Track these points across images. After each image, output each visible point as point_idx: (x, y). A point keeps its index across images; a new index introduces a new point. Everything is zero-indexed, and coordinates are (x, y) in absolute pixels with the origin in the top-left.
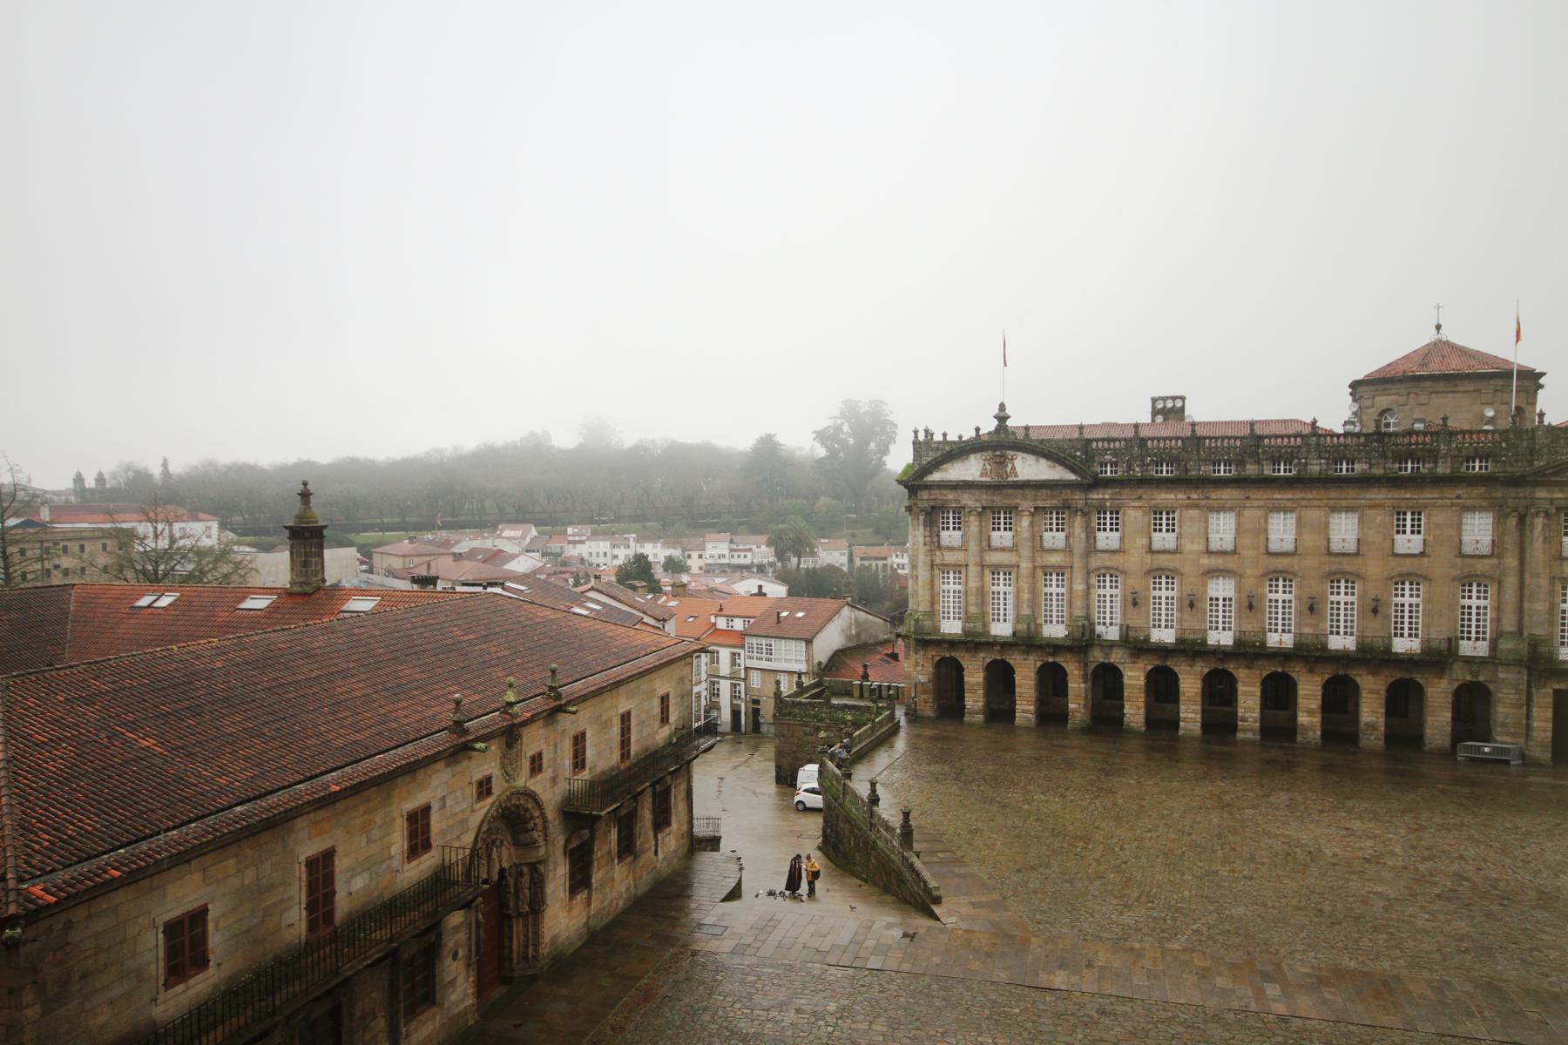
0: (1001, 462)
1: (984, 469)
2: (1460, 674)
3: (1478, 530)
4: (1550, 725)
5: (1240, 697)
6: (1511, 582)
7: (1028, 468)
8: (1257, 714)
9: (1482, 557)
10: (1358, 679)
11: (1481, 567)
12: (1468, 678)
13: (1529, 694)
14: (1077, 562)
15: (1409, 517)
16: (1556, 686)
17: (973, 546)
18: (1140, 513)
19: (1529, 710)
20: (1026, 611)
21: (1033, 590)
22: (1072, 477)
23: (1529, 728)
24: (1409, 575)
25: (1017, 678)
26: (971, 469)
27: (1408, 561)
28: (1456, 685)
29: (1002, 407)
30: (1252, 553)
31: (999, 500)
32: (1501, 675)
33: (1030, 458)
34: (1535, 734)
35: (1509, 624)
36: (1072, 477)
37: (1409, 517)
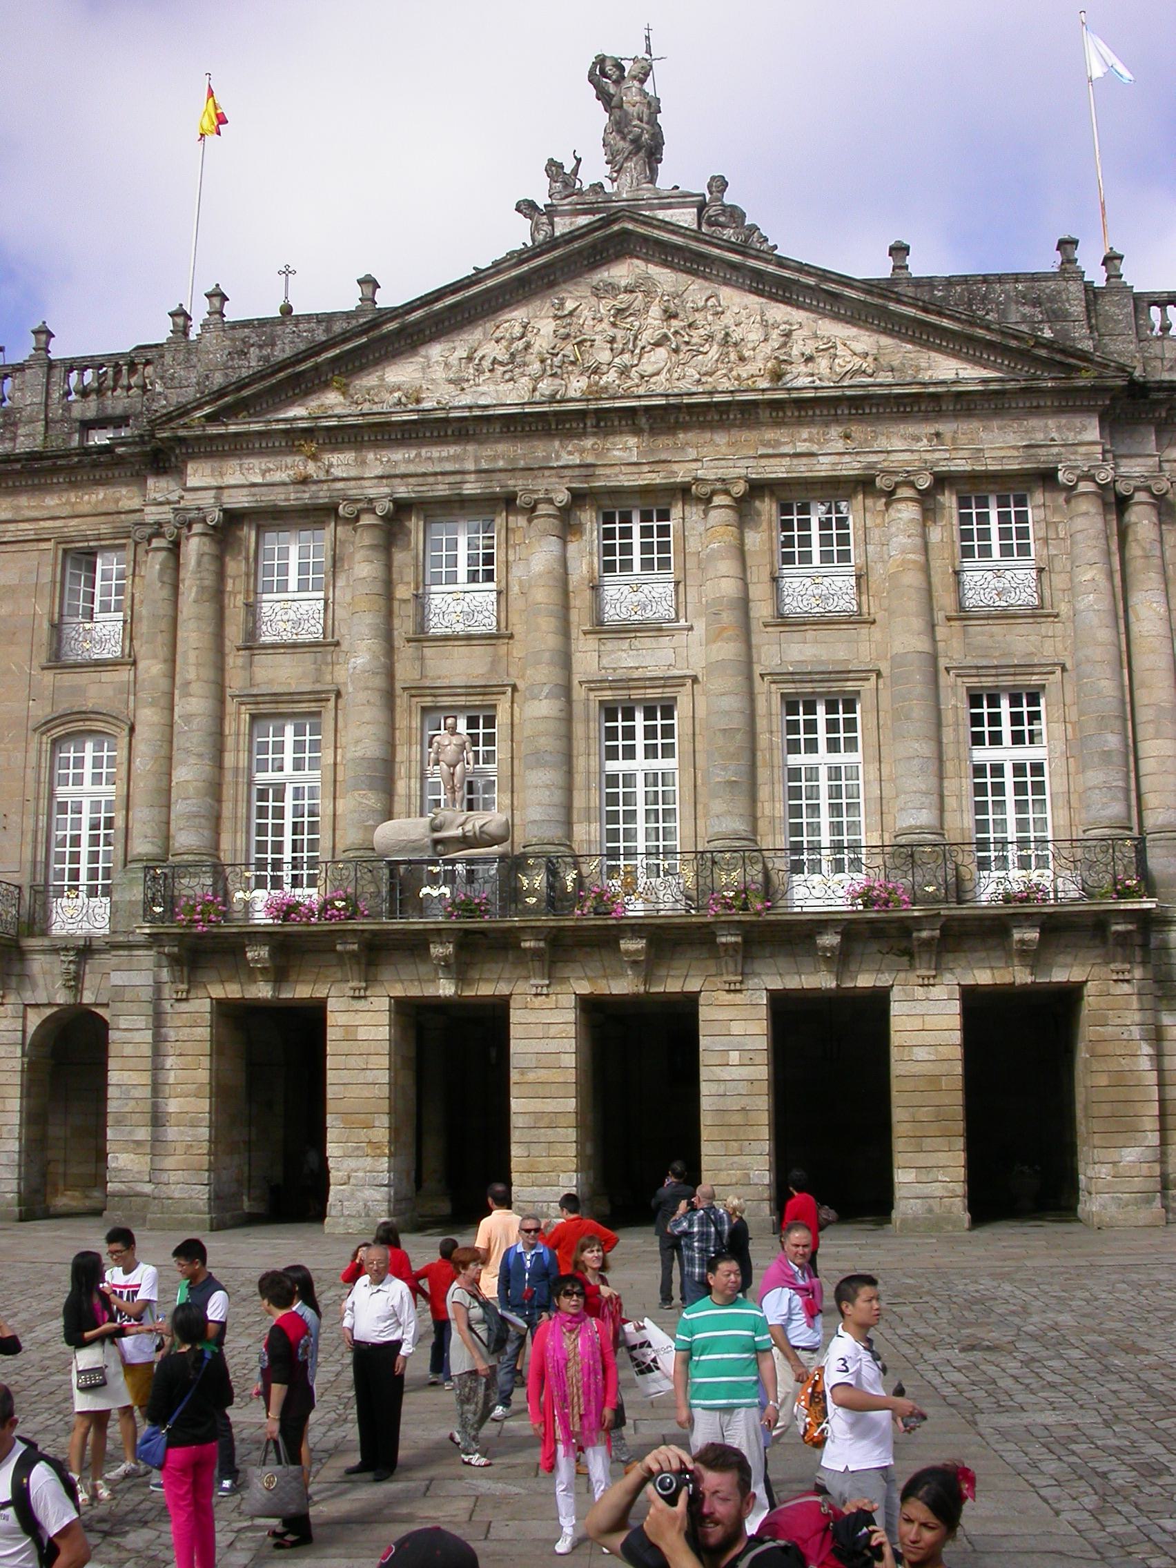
2: (48, 984)
4: (205, 1104)
6: (148, 717)
11: (97, 691)
12: (62, 997)
16: (217, 991)
19: (157, 1068)
23: (157, 1119)
28: (35, 1020)
32: (117, 978)
34: (172, 1133)
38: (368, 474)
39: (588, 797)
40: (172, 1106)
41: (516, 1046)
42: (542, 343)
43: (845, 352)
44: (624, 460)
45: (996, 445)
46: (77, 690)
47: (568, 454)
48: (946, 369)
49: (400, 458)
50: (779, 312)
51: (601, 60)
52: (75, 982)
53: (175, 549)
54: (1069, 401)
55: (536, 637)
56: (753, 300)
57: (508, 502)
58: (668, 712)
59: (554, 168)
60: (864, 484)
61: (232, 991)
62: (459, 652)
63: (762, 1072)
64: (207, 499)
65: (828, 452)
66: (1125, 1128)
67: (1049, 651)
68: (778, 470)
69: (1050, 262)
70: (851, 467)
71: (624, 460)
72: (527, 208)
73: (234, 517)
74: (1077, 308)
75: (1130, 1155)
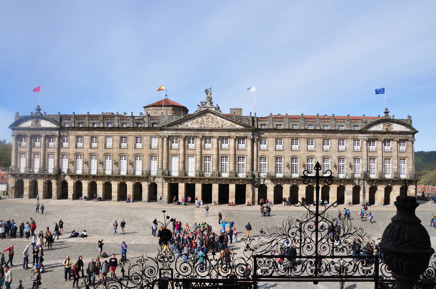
0: (37, 122)
1: (32, 124)
3: (155, 142)
5: (98, 189)
6: (160, 155)
7: (44, 124)
8: (102, 194)
9: (155, 149)
10: (127, 183)
11: (155, 152)
13: (163, 185)
14: (56, 151)
15: (139, 139)
17: (28, 146)
18: (73, 137)
19: (163, 189)
20: (42, 165)
21: (44, 159)
22: (55, 126)
23: (163, 194)
24: (138, 154)
25: (38, 185)
26: (28, 124)
27: (138, 150)
29: (38, 106)
30: (101, 148)
31: (36, 133)
33: (45, 121)
35: (160, 167)
36: (55, 126)
37: (139, 139)
38: (184, 134)
39: (203, 165)
40: (164, 192)
41: (196, 188)
42: (200, 121)
43: (228, 124)
44: (207, 134)
45: (242, 134)
46: (153, 151)
47: (202, 133)
48: (238, 126)
49: (186, 132)
50: (222, 119)
51: (206, 90)
52: (154, 180)
53: (163, 139)
54: (249, 131)
55: (198, 150)
56: (220, 118)
57: (196, 137)
58: (210, 157)
59: (201, 102)
60: (229, 137)
61: (170, 182)
62: (191, 151)
63: (218, 191)
64: (166, 134)
65: (226, 134)
66: (249, 197)
67: (245, 154)
68: (221, 135)
69: (249, 115)
70: (228, 135)
71: (207, 134)
72: (199, 106)
73: (169, 136)
74: (251, 120)
75: (249, 199)
